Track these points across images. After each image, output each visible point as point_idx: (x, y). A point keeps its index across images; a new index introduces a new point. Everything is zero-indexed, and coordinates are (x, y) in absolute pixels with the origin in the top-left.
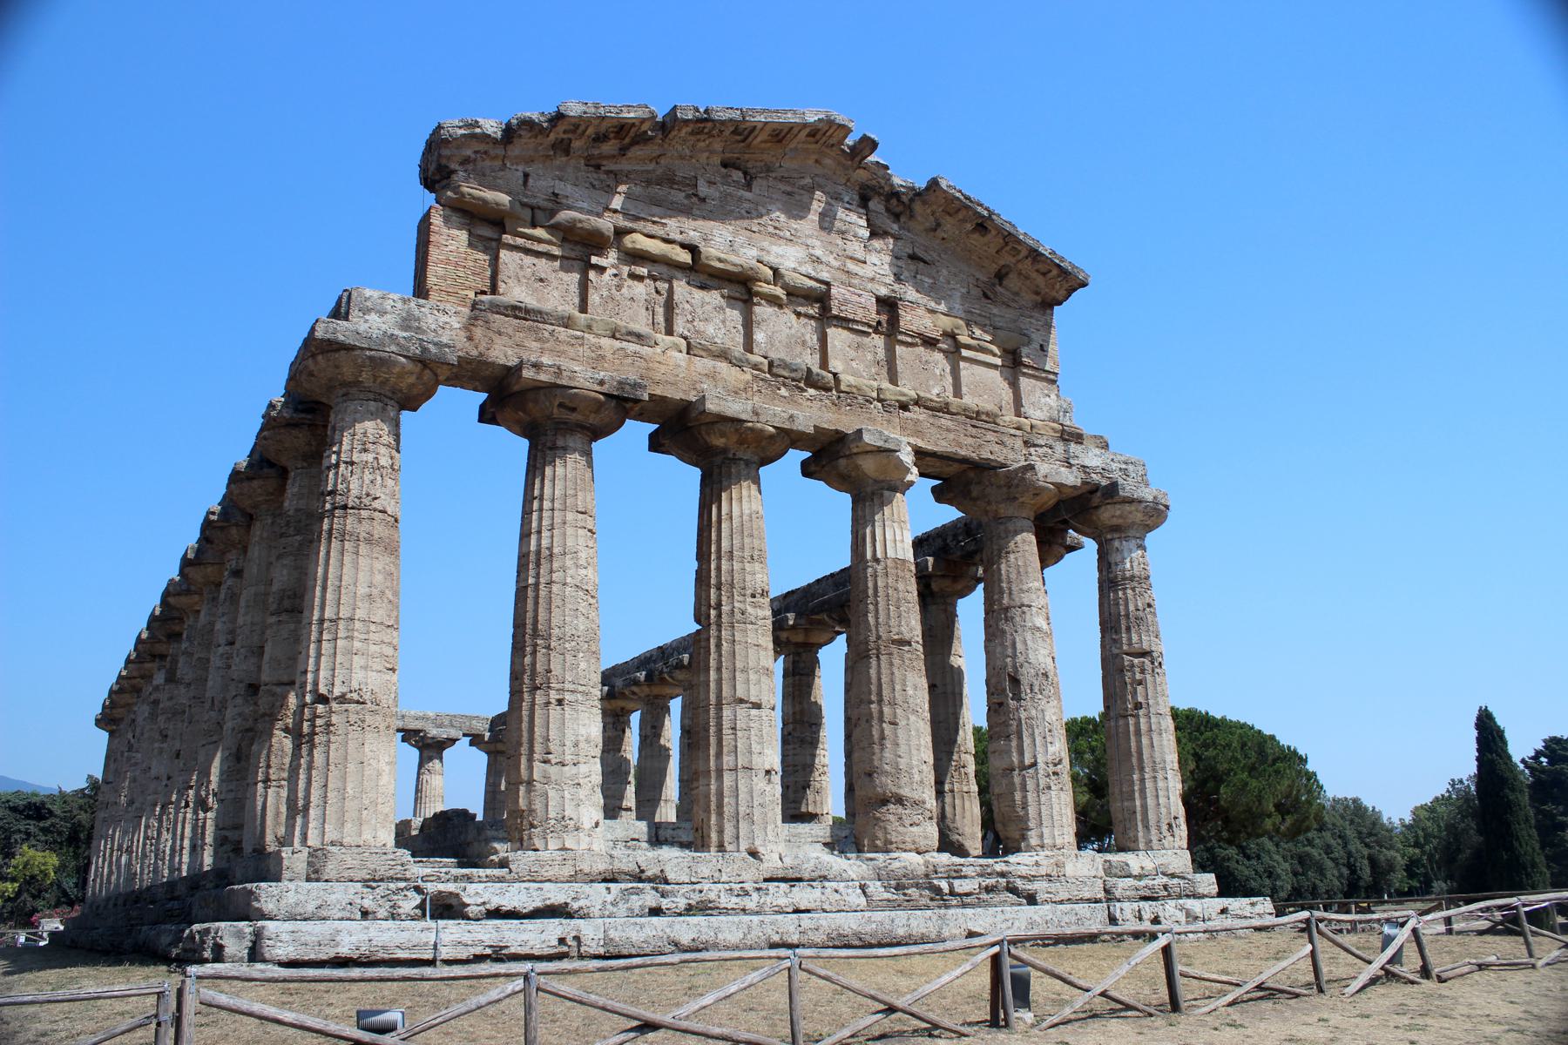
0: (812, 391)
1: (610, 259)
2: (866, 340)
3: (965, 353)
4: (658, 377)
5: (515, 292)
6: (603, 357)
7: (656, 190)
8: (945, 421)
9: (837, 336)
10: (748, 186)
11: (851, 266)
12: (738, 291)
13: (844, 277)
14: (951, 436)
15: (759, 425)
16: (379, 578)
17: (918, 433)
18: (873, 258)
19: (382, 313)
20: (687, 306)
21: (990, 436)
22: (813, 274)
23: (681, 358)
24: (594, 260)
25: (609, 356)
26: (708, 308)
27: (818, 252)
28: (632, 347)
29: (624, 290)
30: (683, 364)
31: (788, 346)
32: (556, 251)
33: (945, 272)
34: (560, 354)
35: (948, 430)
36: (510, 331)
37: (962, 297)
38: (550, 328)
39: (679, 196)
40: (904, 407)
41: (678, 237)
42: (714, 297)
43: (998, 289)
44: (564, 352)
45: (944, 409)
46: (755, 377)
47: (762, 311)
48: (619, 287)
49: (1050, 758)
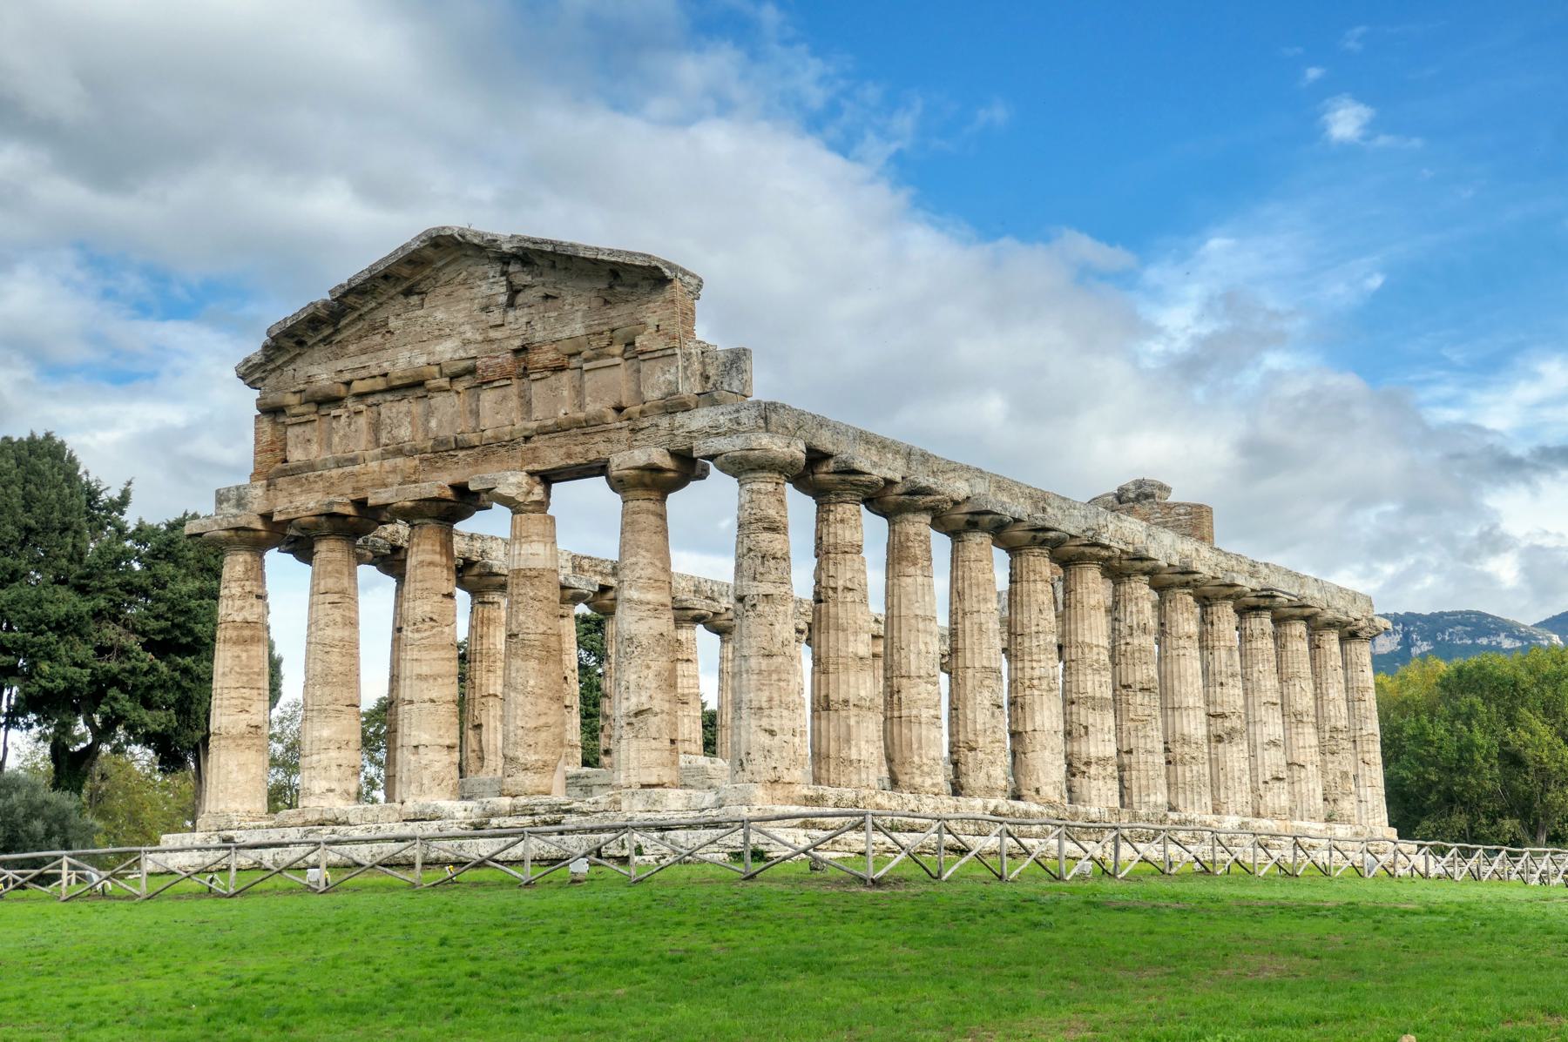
0: (461, 454)
1: (351, 404)
2: (509, 389)
3: (586, 366)
4: (361, 485)
5: (296, 455)
7: (365, 343)
8: (560, 439)
9: (488, 397)
10: (422, 306)
11: (493, 334)
12: (420, 392)
13: (486, 347)
16: (229, 662)
17: (535, 459)
18: (511, 314)
19: (228, 500)
21: (597, 438)
22: (464, 355)
23: (374, 465)
24: (334, 412)
27: (469, 335)
31: (452, 422)
32: (312, 417)
33: (570, 300)
34: (310, 491)
37: (584, 316)
39: (378, 338)
41: (375, 372)
42: (404, 406)
43: (619, 289)
45: (560, 429)
46: (422, 460)
47: (438, 400)
49: (623, 711)
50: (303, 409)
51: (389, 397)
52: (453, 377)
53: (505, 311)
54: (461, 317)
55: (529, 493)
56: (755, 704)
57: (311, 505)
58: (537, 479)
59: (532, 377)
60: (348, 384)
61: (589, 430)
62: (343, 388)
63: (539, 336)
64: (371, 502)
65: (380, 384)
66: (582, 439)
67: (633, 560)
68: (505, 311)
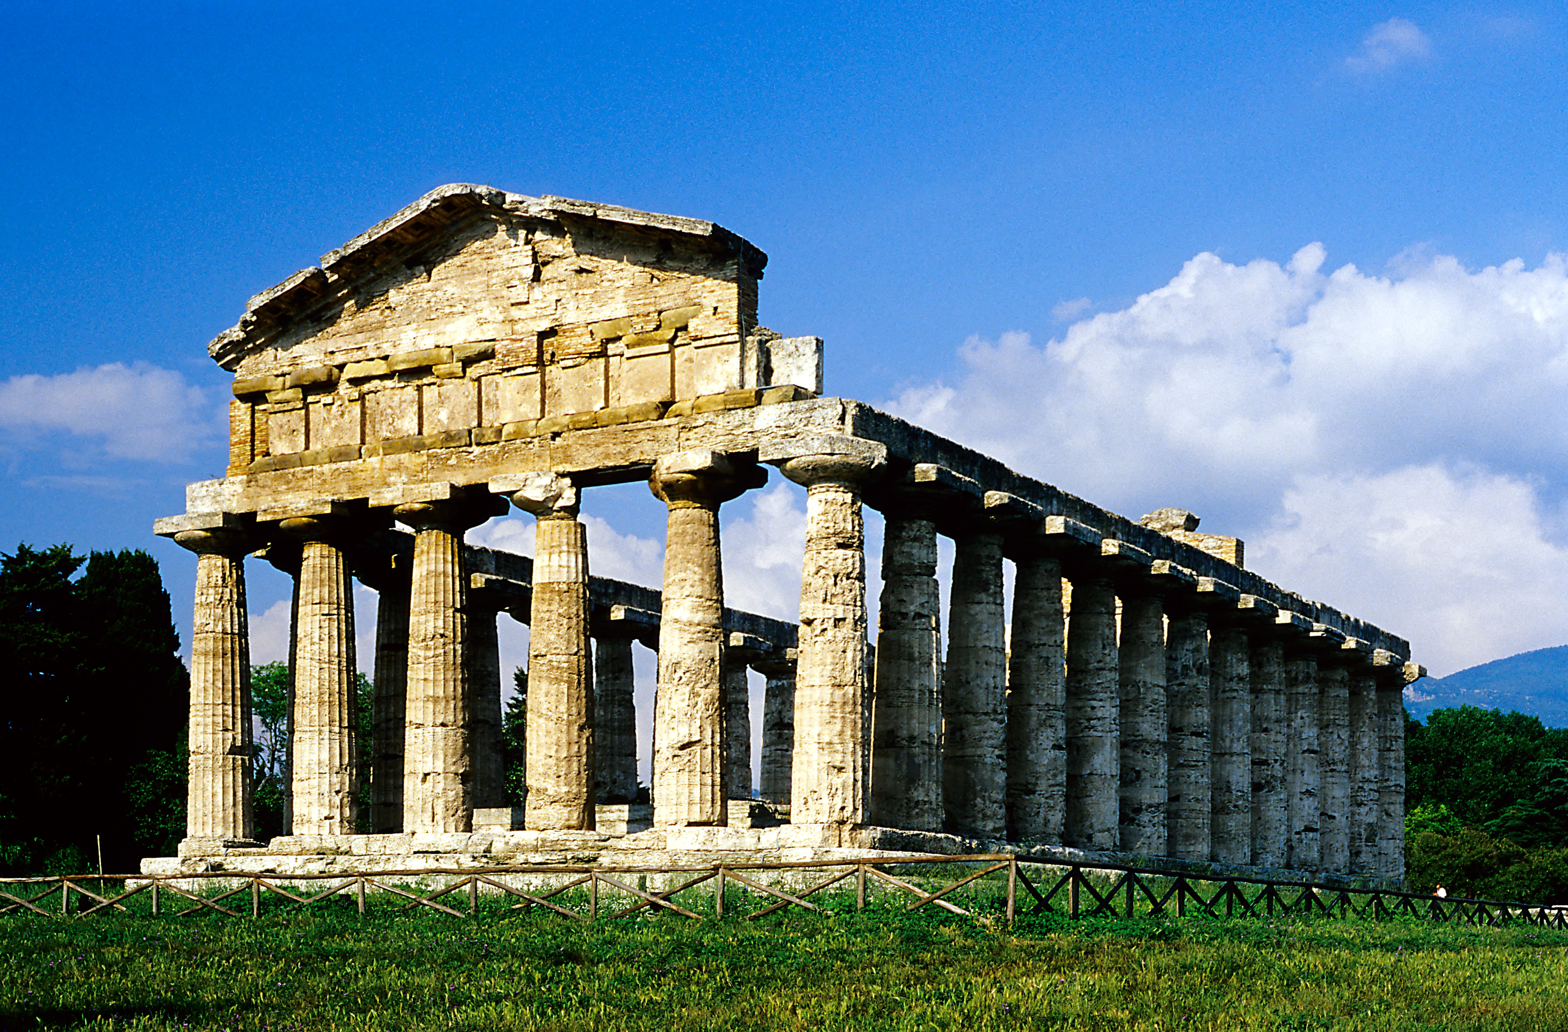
0: (476, 450)
1: (344, 388)
4: (359, 483)
5: (280, 447)
6: (324, 481)
11: (515, 313)
13: (508, 327)
14: (600, 450)
15: (407, 507)
17: (568, 459)
20: (389, 411)
21: (642, 436)
25: (329, 478)
26: (404, 405)
27: (485, 314)
28: (344, 465)
29: (346, 416)
30: (377, 466)
35: (597, 446)
36: (269, 483)
37: (626, 295)
38: (292, 470)
40: (555, 435)
42: (410, 392)
44: (301, 486)
45: (594, 423)
48: (342, 415)
50: (289, 394)
51: (389, 383)
52: (467, 362)
53: (531, 288)
54: (477, 292)
55: (558, 496)
56: (826, 738)
57: (302, 505)
58: (567, 481)
59: (563, 364)
60: (341, 367)
61: (630, 426)
62: (336, 371)
63: (570, 316)
64: (372, 503)
65: (381, 368)
66: (622, 437)
67: (682, 575)
68: (531, 288)
